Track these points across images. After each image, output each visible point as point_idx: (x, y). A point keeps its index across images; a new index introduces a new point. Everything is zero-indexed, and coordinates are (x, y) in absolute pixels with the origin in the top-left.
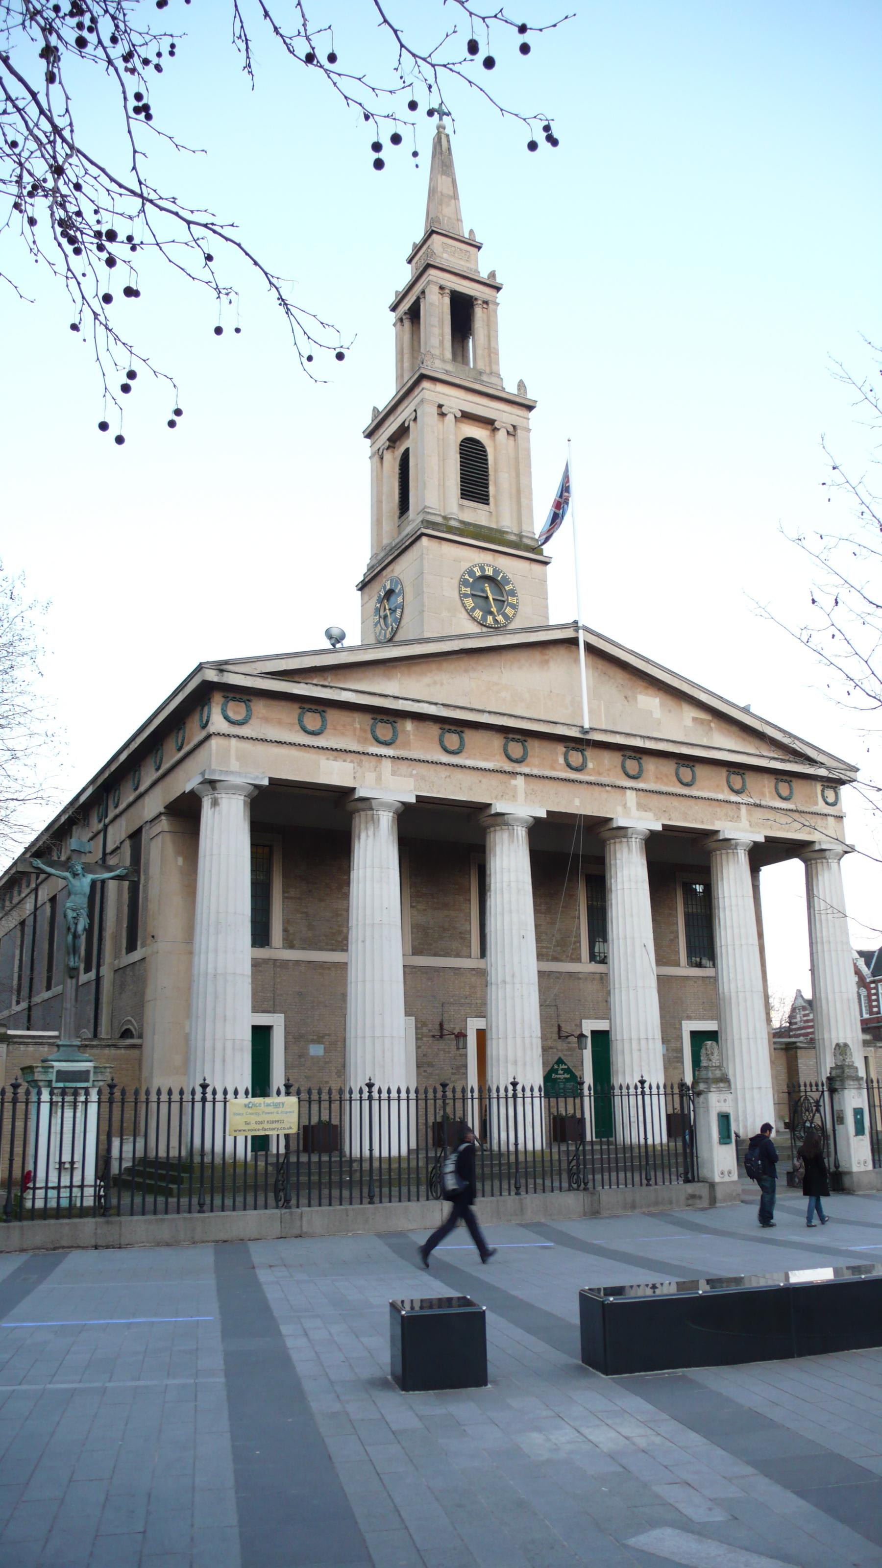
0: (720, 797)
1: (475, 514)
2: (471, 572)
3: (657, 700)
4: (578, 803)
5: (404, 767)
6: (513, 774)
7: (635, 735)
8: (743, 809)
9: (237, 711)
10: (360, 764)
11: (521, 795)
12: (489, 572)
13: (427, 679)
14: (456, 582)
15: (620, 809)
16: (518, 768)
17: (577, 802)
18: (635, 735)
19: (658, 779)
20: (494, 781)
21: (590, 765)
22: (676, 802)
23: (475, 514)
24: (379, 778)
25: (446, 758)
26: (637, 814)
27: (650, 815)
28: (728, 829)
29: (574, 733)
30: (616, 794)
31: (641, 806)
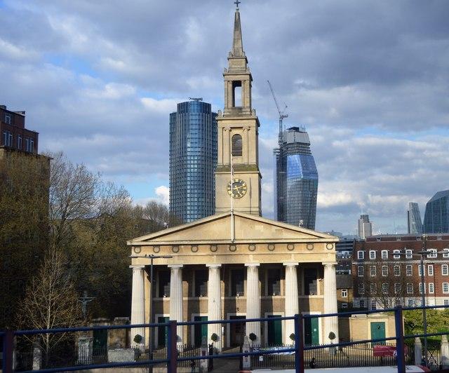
1: (238, 161)
5: (180, 257)
6: (213, 255)
8: (293, 255)
9: (137, 250)
12: (237, 181)
13: (187, 233)
14: (226, 186)
15: (247, 261)
16: (214, 253)
19: (261, 250)
20: (207, 258)
21: (237, 249)
22: (267, 256)
23: (238, 161)
25: (192, 254)
26: (252, 261)
27: (257, 261)
30: (246, 257)
31: (256, 259)
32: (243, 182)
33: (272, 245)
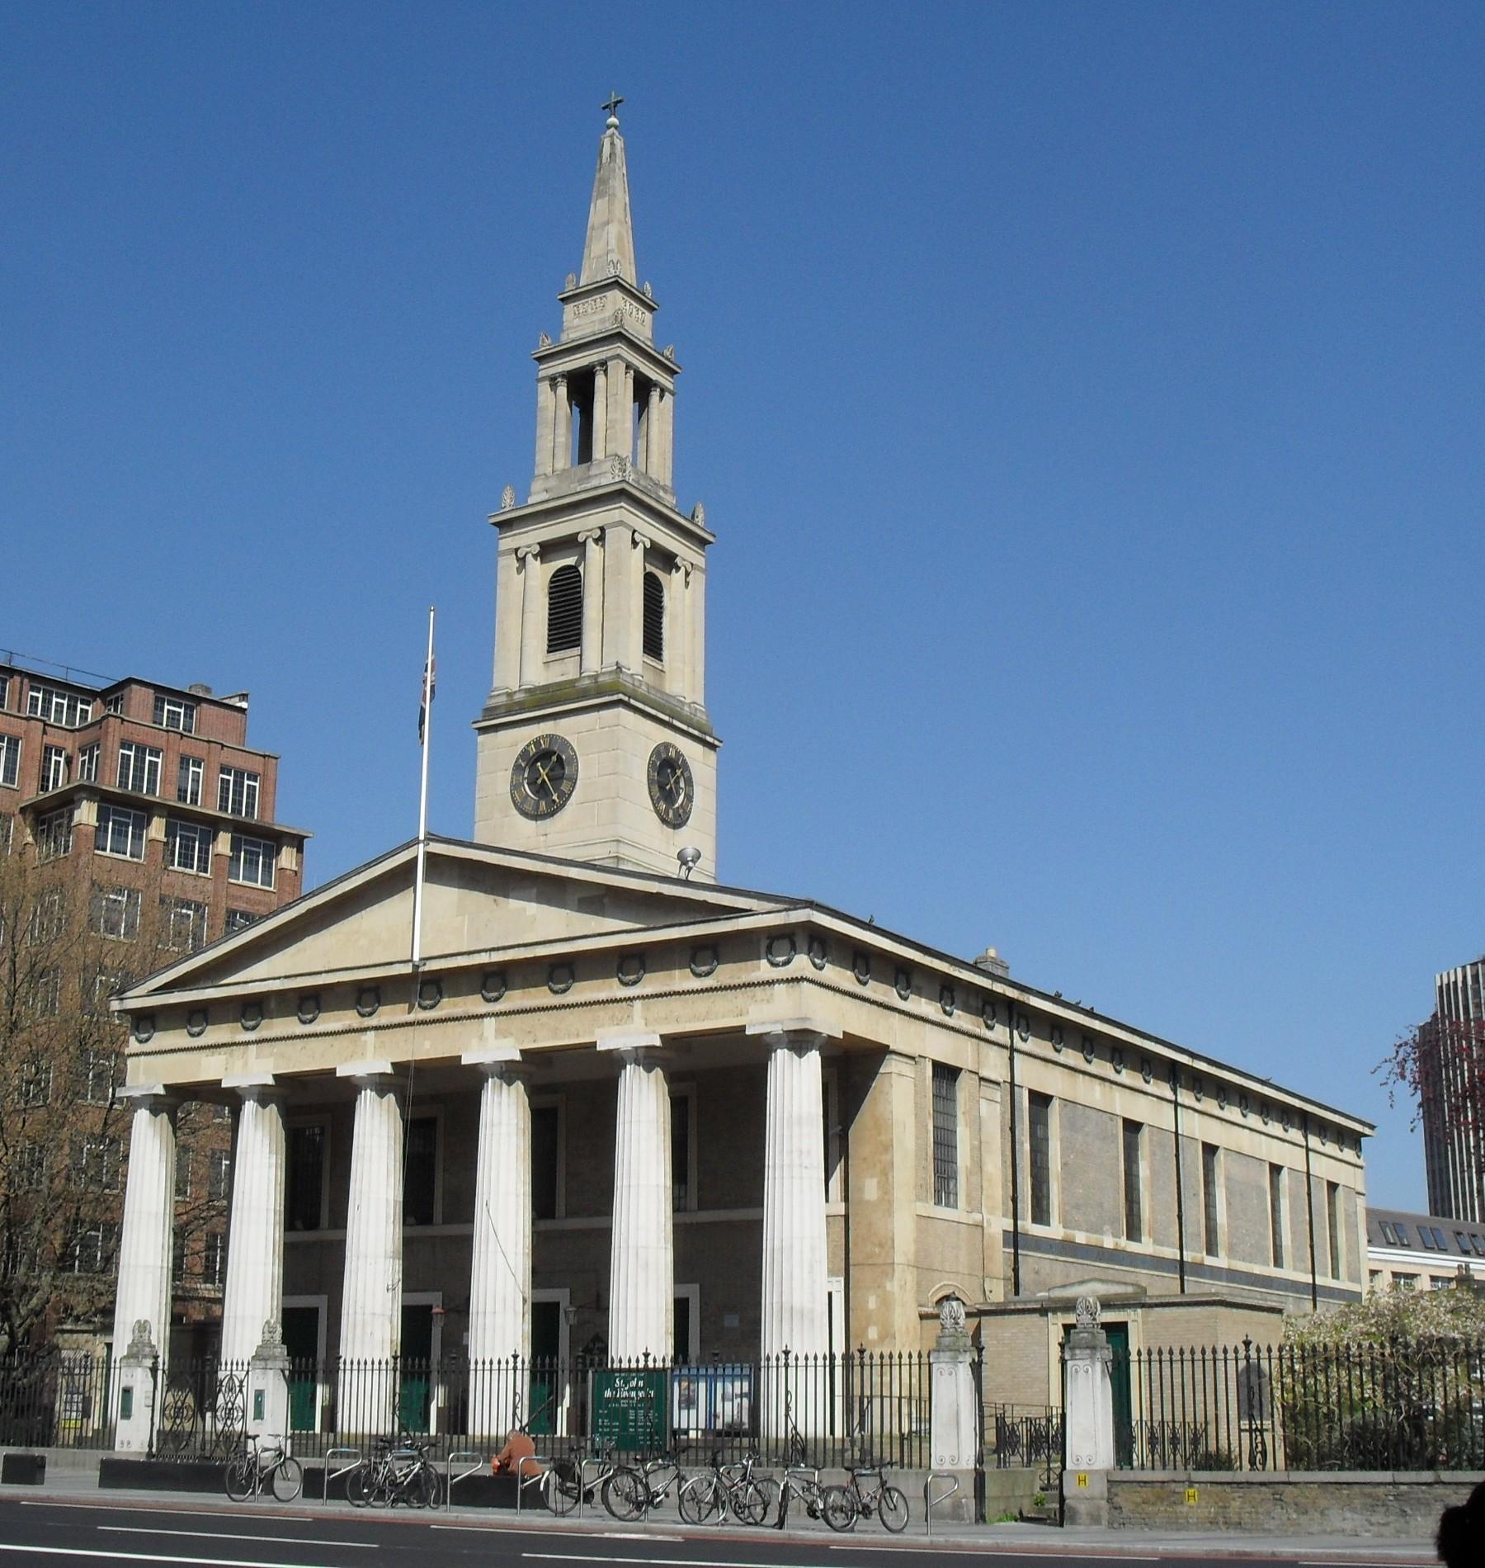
0: (603, 996)
1: (564, 669)
2: (525, 752)
3: (535, 891)
4: (427, 1046)
6: (366, 1029)
7: (479, 952)
10: (231, 1055)
11: (370, 1048)
15: (475, 1042)
17: (427, 1045)
18: (479, 952)
24: (246, 1064)
28: (612, 1036)
29: (407, 969)
31: (501, 1033)
32: (566, 744)
33: (561, 970)
